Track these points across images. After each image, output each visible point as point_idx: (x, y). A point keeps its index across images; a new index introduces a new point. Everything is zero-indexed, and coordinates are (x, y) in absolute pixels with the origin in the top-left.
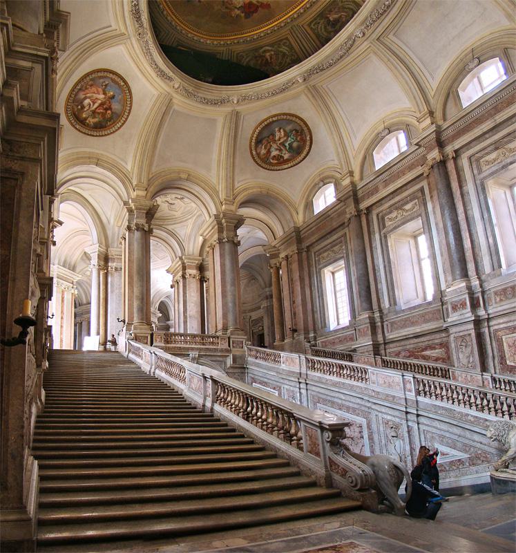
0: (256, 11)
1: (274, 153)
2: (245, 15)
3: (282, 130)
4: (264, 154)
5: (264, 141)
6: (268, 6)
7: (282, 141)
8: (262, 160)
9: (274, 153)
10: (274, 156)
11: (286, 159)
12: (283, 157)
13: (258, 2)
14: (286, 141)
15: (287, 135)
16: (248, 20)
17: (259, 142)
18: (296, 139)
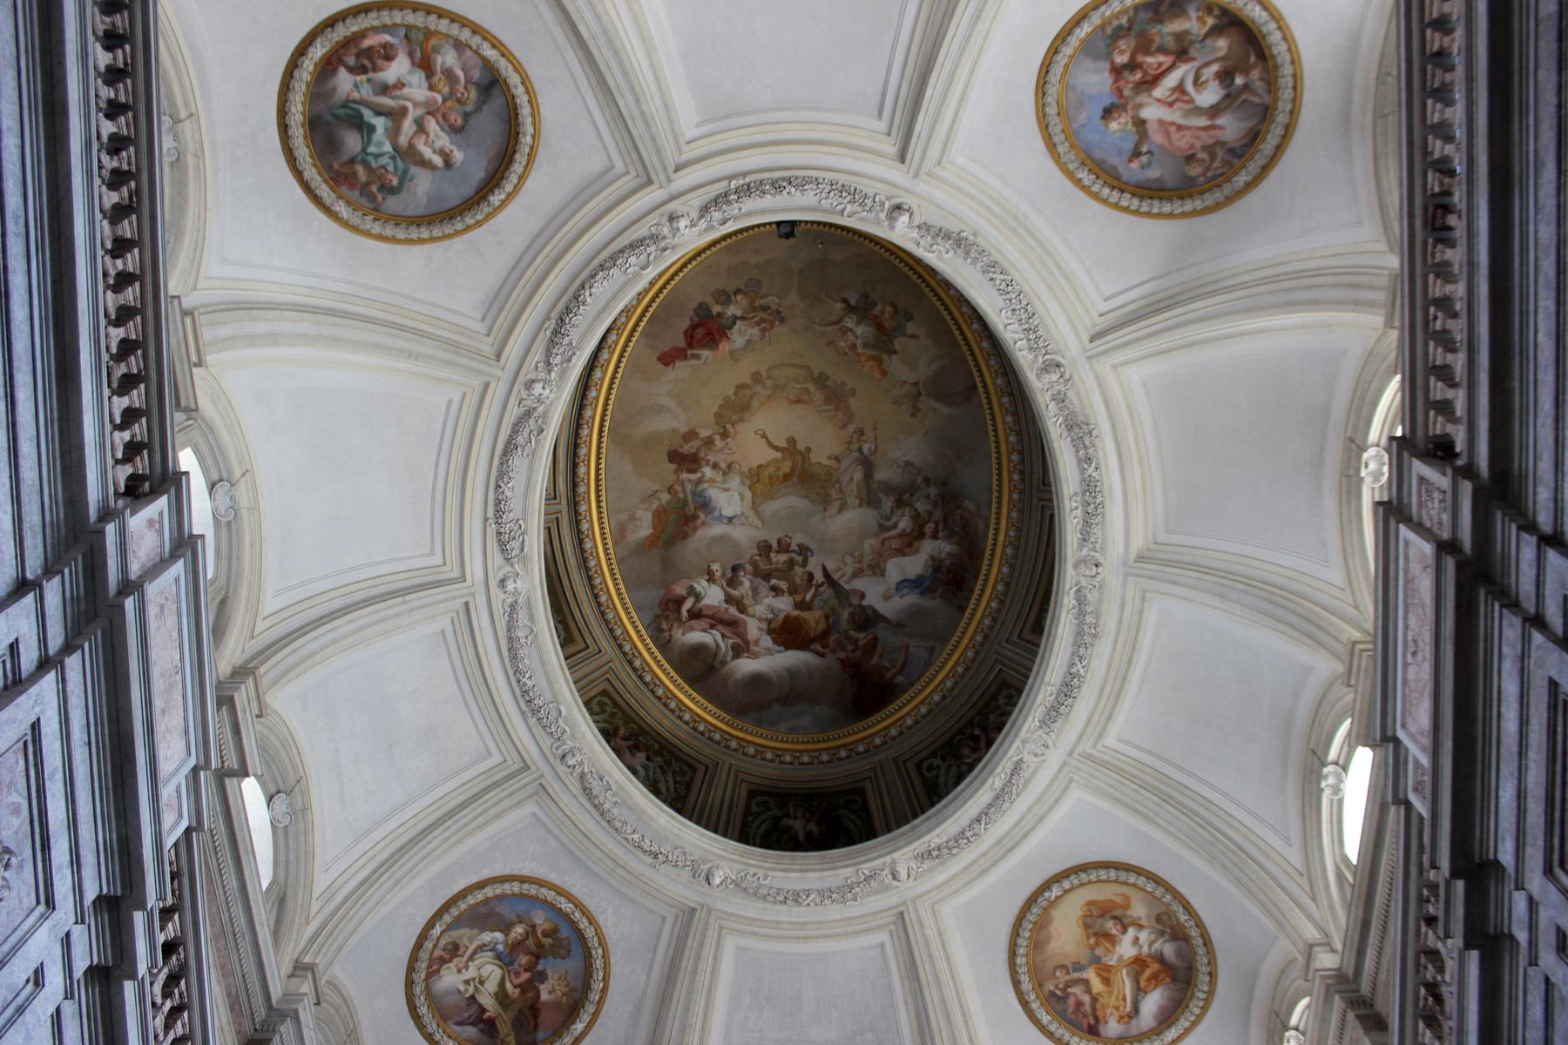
0: (690, 334)
1: (398, 68)
2: (709, 311)
3: (438, 160)
4: (436, 50)
5: (473, 95)
6: (667, 359)
7: (408, 125)
8: (429, 34)
9: (398, 68)
10: (389, 58)
11: (334, 71)
12: (351, 70)
13: (697, 357)
14: (393, 134)
15: (409, 155)
16: (695, 305)
17: (491, 84)
18: (367, 166)
